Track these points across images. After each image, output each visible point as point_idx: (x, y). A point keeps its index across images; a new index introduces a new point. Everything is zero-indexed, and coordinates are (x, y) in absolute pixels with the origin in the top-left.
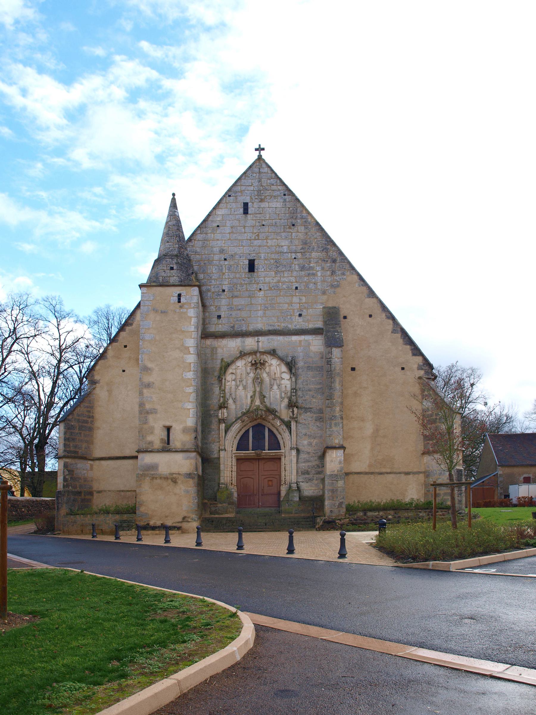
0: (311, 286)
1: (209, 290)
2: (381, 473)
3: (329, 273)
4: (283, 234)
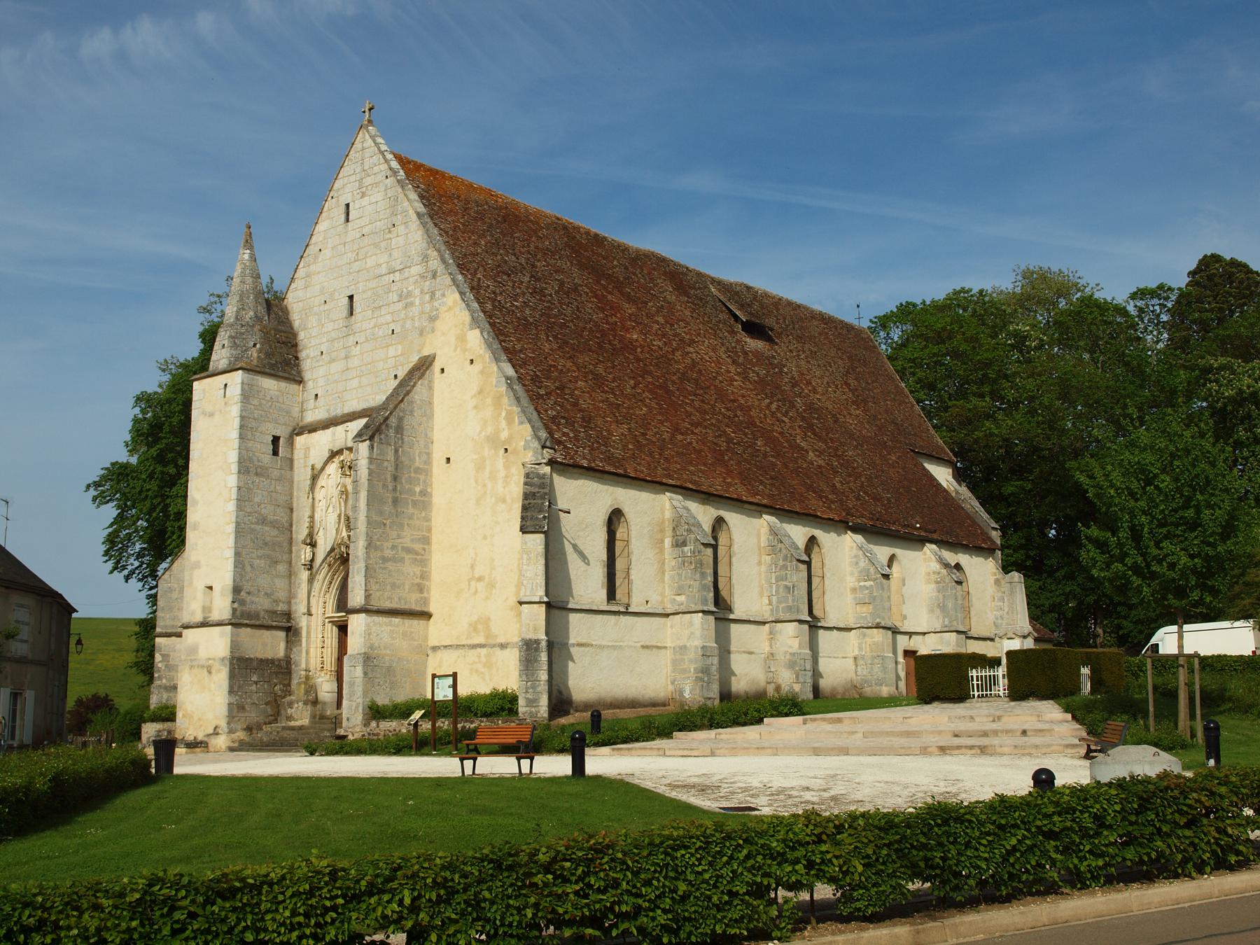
0: (408, 324)
1: (308, 357)
2: (474, 647)
3: (427, 297)
4: (383, 245)
